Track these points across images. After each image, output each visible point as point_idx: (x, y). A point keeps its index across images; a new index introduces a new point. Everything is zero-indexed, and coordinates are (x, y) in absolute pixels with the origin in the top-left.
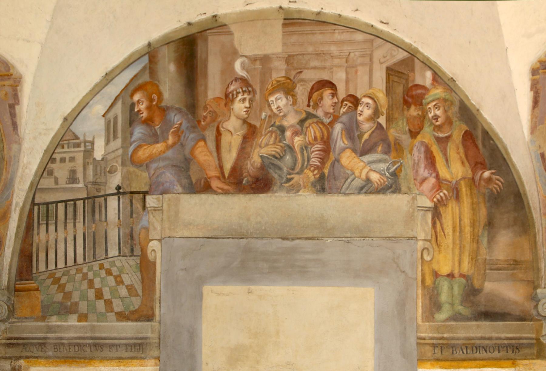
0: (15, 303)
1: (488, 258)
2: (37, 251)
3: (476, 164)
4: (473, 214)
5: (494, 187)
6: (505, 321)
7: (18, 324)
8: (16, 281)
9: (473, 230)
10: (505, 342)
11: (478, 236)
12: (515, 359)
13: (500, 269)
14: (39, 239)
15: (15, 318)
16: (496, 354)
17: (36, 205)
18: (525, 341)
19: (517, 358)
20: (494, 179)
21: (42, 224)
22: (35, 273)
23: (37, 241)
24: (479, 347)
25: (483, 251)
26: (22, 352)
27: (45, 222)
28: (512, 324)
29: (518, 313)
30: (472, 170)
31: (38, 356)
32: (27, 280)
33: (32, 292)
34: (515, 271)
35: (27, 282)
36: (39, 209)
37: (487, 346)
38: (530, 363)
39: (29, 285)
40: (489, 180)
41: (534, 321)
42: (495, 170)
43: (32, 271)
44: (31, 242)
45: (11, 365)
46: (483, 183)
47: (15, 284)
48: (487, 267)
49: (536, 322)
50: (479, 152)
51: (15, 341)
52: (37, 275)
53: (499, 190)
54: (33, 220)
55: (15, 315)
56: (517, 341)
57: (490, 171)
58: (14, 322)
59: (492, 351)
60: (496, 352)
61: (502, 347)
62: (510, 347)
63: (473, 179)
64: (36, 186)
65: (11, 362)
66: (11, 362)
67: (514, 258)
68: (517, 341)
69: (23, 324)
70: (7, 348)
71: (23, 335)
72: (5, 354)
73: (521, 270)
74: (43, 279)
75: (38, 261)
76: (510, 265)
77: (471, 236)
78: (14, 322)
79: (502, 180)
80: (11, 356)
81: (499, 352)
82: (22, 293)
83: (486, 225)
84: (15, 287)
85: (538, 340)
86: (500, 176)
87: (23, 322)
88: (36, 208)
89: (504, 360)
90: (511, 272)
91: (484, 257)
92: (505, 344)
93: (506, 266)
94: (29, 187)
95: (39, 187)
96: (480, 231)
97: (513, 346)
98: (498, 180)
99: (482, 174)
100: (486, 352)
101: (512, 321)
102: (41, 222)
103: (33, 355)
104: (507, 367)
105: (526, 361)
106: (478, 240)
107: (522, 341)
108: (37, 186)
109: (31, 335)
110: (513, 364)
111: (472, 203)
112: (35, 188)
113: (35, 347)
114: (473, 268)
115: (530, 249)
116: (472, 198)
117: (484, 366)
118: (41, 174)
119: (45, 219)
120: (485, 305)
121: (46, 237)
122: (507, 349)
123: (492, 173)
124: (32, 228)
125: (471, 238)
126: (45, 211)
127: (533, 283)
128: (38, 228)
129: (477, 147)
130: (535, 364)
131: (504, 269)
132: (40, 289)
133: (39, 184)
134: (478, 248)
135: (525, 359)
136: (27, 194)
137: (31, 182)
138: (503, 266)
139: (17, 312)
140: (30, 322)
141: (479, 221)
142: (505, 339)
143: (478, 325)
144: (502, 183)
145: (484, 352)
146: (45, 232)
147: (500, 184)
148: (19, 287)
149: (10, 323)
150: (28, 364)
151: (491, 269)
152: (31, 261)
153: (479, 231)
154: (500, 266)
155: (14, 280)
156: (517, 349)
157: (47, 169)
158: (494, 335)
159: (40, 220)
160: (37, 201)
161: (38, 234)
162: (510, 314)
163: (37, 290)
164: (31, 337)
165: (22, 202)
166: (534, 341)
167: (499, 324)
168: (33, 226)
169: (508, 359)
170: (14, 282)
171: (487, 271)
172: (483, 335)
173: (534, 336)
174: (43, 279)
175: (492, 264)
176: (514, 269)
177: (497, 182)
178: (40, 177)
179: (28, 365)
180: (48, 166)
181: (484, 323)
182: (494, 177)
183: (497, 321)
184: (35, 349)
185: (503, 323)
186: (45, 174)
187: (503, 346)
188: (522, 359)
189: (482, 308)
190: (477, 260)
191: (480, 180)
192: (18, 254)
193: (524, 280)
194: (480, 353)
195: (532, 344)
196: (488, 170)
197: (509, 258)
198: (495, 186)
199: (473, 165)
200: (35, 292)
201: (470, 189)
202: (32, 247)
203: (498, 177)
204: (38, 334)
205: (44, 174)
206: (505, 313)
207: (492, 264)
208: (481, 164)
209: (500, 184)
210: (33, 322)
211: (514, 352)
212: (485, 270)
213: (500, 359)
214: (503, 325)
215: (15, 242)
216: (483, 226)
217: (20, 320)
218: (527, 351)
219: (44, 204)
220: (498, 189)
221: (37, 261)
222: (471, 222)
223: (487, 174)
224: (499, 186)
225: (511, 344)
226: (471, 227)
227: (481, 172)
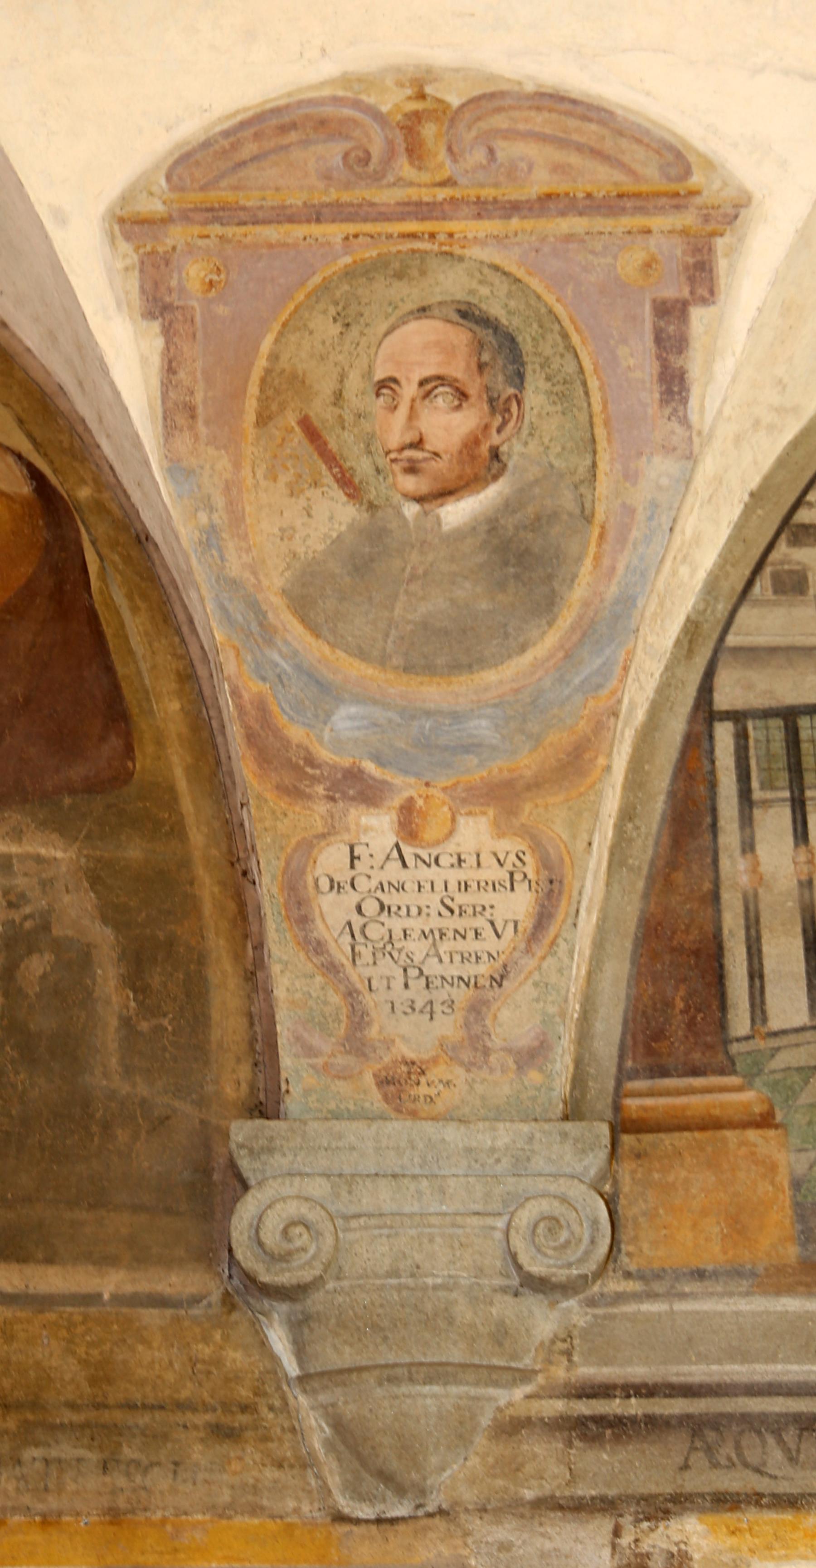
0: (626, 1189)
2: (748, 928)
7: (647, 1307)
8: (622, 1075)
14: (755, 868)
15: (628, 1275)
17: (721, 720)
21: (766, 804)
22: (747, 1038)
23: (744, 880)
26: (686, 1467)
27: (787, 794)
31: (803, 1495)
32: (695, 1072)
33: (728, 1134)
35: (698, 1082)
36: (742, 736)
39: (708, 1098)
43: (723, 1025)
44: (707, 886)
45: (614, 1546)
47: (619, 1093)
51: (635, 1407)
52: (759, 1044)
54: (713, 785)
55: (625, 1259)
58: (619, 1298)
64: (715, 636)
65: (617, 1532)
66: (617, 1532)
69: (681, 1306)
70: (577, 1443)
71: (685, 1368)
72: (572, 1482)
74: (799, 1069)
75: (761, 977)
78: (619, 1298)
80: (612, 1492)
82: (667, 1140)
84: (617, 1108)
87: (683, 1296)
88: (724, 733)
94: (678, 643)
95: (732, 640)
102: (757, 794)
103: (763, 1485)
108: (722, 639)
109: (736, 1367)
112: (711, 645)
113: (771, 1440)
118: (740, 587)
119: (783, 778)
121: (795, 863)
124: (709, 820)
126: (778, 745)
128: (746, 820)
132: (779, 1117)
133: (734, 629)
136: (667, 668)
137: (688, 619)
139: (635, 1239)
140: (731, 1294)
146: (790, 840)
148: (645, 1109)
149: (591, 1303)
150: (732, 1541)
152: (720, 978)
155: (613, 1070)
157: (768, 570)
159: (755, 784)
160: (722, 700)
161: (748, 847)
163: (765, 1121)
164: (745, 1379)
165: (647, 705)
168: (714, 811)
170: (611, 1084)
174: (795, 1064)
178: (734, 599)
179: (732, 1549)
180: (774, 556)
184: (777, 1455)
186: (762, 587)
192: (629, 945)
200: (752, 1135)
202: (718, 911)
204: (786, 1360)
205: (757, 589)
210: (748, 1294)
215: (608, 884)
217: (658, 1287)
219: (767, 714)
221: (756, 975)
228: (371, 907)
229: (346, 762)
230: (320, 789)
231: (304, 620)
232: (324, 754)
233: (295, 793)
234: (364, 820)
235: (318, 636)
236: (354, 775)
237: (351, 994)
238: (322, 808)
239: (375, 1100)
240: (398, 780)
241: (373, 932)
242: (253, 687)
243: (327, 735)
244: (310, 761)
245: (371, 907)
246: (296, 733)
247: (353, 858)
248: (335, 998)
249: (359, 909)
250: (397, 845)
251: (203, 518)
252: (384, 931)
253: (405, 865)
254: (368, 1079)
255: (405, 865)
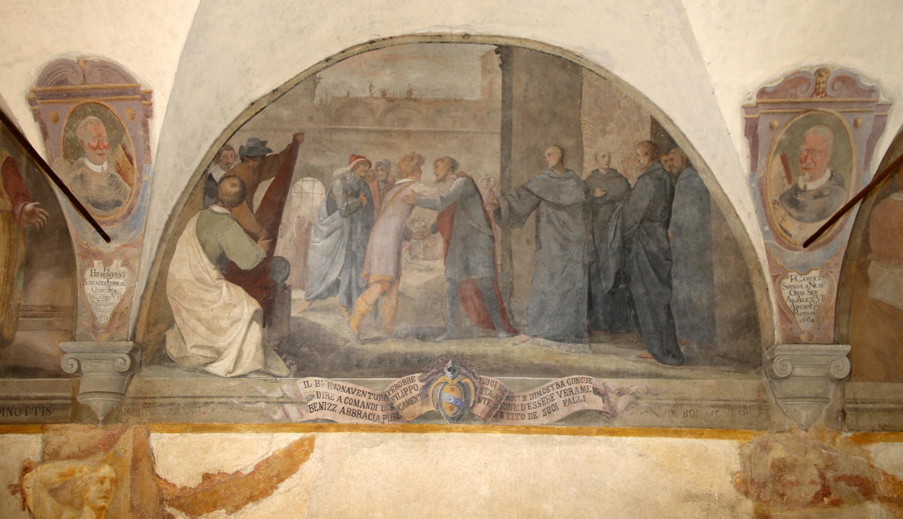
1: (22, 303)
3: (18, 195)
4: (10, 252)
5: (37, 221)
6: (36, 378)
9: (8, 271)
10: (35, 402)
11: (13, 278)
12: (45, 423)
13: (35, 317)
16: (23, 417)
18: (58, 401)
19: (47, 422)
20: (38, 212)
24: (4, 408)
25: (17, 295)
28: (44, 381)
29: (51, 369)
30: (12, 202)
34: (52, 319)
37: (13, 408)
38: (62, 427)
40: (32, 213)
41: (70, 378)
42: (39, 201)
46: (24, 217)
48: (21, 314)
49: (72, 379)
50: (22, 182)
53: (42, 225)
56: (48, 402)
57: (33, 203)
59: (18, 414)
60: (23, 415)
61: (30, 408)
62: (40, 410)
63: (13, 212)
67: (52, 304)
68: (48, 402)
73: (59, 317)
76: (47, 311)
77: (4, 278)
79: (46, 213)
81: (26, 415)
83: (23, 266)
85: (74, 399)
86: (45, 210)
89: (32, 423)
90: (48, 319)
91: (18, 302)
92: (35, 404)
93: (42, 313)
96: (16, 272)
97: (43, 408)
98: (42, 213)
99: (24, 206)
100: (11, 414)
101: (44, 378)
104: (34, 433)
105: (57, 425)
106: (12, 283)
107: (54, 402)
110: (42, 428)
111: (10, 240)
114: (4, 315)
115: (72, 292)
116: (10, 235)
117: (7, 432)
120: (15, 359)
122: (36, 411)
123: (36, 206)
125: (4, 281)
127: (71, 332)
129: (19, 176)
130: (67, 429)
131: (41, 316)
134: (12, 292)
135: (57, 423)
138: (39, 312)
141: (16, 261)
142: (33, 399)
143: (4, 382)
144: (46, 217)
145: (9, 414)
147: (44, 218)
151: (25, 317)
153: (14, 272)
154: (36, 312)
156: (48, 410)
158: (23, 394)
162: (41, 369)
166: (69, 401)
167: (29, 381)
169: (36, 423)
171: (20, 319)
172: (9, 394)
173: (69, 395)
175: (26, 311)
176: (51, 316)
177: (41, 215)
181: (12, 380)
182: (38, 209)
183: (27, 378)
185: (34, 380)
187: (31, 407)
188: (52, 423)
189: (11, 363)
190: (9, 306)
191: (21, 213)
193: (60, 330)
194: (3, 415)
195: (66, 404)
196: (31, 202)
197: (46, 304)
198: (39, 220)
199: (13, 197)
201: (9, 224)
203: (42, 210)
206: (37, 368)
207: (26, 311)
208: (24, 195)
209: (44, 218)
211: (45, 414)
212: (17, 318)
213: (27, 423)
214: (34, 382)
216: (19, 266)
218: (59, 413)
220: (42, 223)
222: (6, 262)
223: (29, 206)
224: (43, 221)
225: (41, 404)
226: (5, 267)
227: (22, 205)
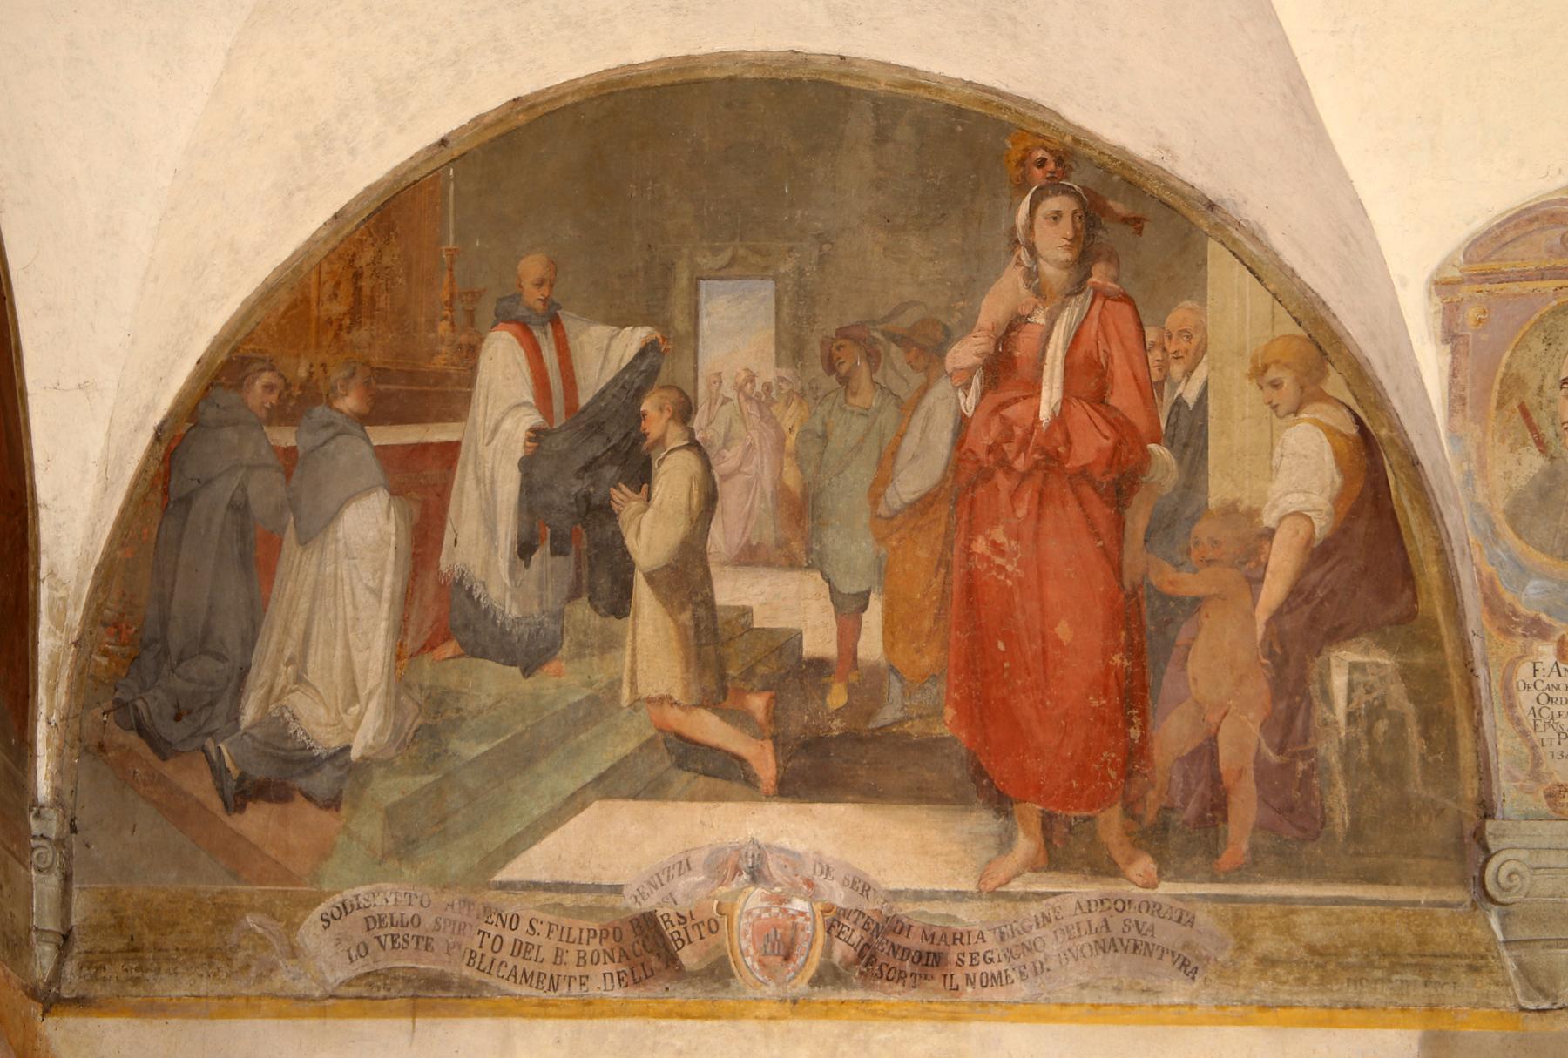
228: (1543, 699)
229: (1532, 613)
230: (1519, 630)
231: (1513, 528)
232: (1522, 609)
233: (1507, 633)
234: (1540, 648)
235: (1520, 538)
236: (1536, 621)
237: (1533, 748)
238: (1520, 641)
239: (1544, 807)
240: (1557, 624)
241: (1545, 713)
242: (1488, 569)
243: (1523, 597)
244: (1515, 614)
245: (1543, 699)
246: (1508, 597)
247: (1535, 670)
248: (1526, 750)
249: (1538, 699)
250: (1556, 663)
251: (1465, 466)
252: (1549, 712)
253: (1560, 675)
254: (1541, 794)
255: (1560, 675)
